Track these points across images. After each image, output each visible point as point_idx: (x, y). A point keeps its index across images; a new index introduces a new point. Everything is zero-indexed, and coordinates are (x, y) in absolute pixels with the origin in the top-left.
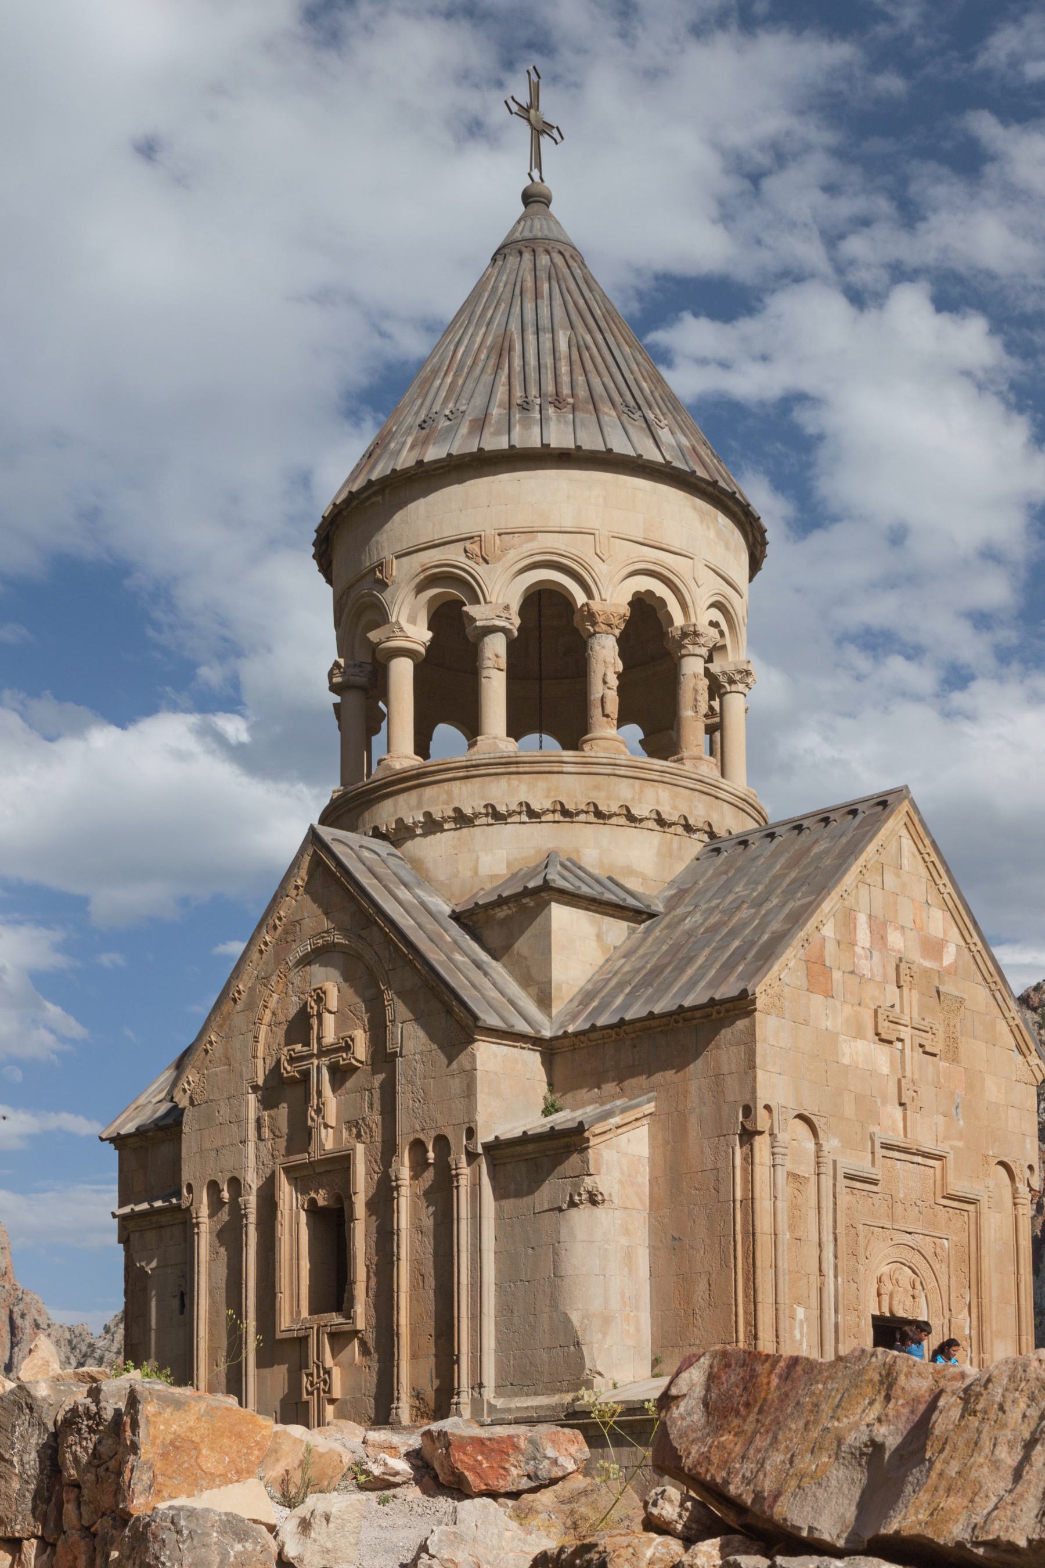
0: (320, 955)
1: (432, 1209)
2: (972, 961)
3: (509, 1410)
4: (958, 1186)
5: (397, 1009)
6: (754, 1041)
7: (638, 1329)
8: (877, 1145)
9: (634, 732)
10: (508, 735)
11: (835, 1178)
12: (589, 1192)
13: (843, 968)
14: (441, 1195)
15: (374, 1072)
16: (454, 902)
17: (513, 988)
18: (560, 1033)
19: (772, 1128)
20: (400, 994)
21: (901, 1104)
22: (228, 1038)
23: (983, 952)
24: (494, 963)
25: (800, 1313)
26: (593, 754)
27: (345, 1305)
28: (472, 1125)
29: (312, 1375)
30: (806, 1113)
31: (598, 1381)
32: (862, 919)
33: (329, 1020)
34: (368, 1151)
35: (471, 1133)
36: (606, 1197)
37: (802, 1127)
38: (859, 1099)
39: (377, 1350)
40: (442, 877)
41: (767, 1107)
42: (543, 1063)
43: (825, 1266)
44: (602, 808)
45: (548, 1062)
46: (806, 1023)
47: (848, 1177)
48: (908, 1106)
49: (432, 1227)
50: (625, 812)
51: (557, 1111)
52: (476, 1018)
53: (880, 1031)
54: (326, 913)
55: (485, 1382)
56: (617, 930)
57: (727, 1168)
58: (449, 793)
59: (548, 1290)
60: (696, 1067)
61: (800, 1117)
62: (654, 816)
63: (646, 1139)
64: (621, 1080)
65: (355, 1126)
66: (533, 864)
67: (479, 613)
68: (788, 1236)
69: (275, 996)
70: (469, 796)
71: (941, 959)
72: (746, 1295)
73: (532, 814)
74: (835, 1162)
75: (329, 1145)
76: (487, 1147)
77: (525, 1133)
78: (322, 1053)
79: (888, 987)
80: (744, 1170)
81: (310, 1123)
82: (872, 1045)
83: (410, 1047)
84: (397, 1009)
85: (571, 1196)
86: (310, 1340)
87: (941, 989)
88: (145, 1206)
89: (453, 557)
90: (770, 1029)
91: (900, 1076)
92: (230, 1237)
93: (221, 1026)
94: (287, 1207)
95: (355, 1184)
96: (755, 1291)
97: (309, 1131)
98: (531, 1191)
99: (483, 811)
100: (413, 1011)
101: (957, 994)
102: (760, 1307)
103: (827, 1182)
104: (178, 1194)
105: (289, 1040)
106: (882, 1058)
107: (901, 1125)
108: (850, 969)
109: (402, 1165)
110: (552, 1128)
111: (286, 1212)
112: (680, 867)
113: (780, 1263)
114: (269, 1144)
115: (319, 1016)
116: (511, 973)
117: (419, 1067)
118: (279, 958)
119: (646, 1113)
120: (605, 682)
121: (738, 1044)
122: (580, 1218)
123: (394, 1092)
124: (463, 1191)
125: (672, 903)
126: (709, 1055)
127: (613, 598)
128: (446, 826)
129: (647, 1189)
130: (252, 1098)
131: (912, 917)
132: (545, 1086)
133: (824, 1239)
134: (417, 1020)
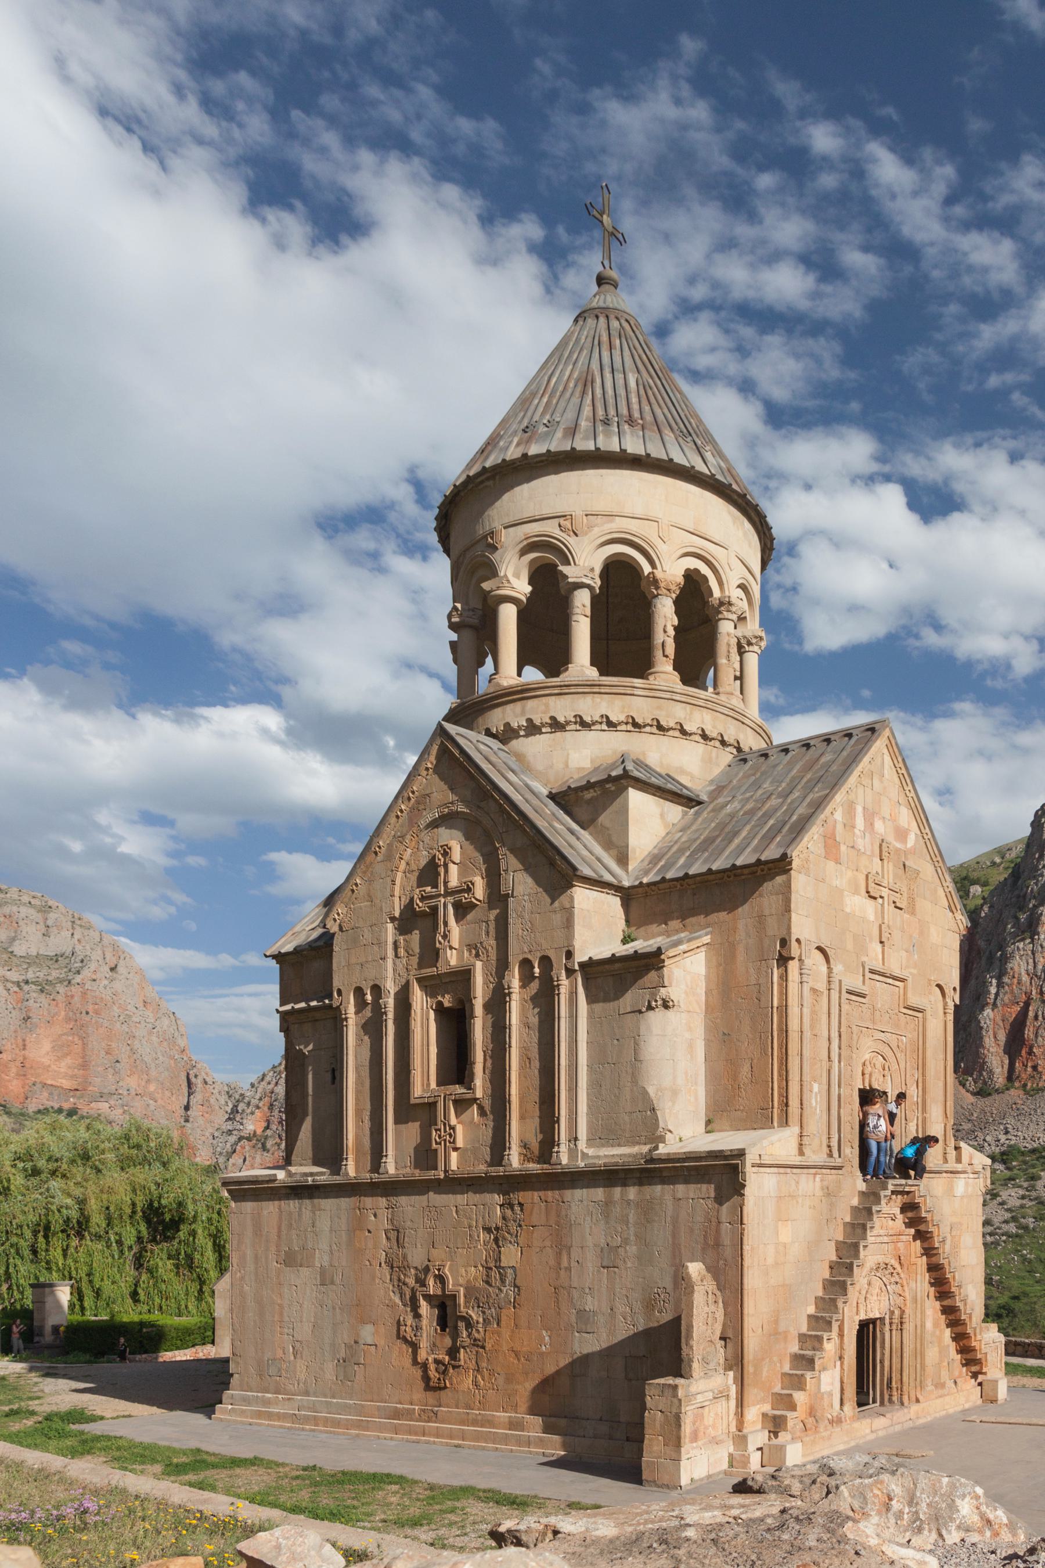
0: (446, 820)
1: (537, 1010)
3: (598, 1157)
4: (914, 1000)
5: (510, 862)
7: (696, 1099)
8: (867, 970)
10: (592, 664)
14: (545, 1000)
15: (490, 908)
16: (549, 786)
17: (598, 850)
18: (637, 883)
19: (801, 955)
20: (512, 851)
21: (881, 942)
22: (370, 881)
24: (582, 831)
25: (816, 1087)
27: (466, 1080)
28: (571, 948)
29: (440, 1130)
33: (453, 869)
35: (569, 955)
37: (819, 955)
39: (492, 1112)
41: (798, 941)
42: (622, 905)
45: (626, 904)
49: (537, 1024)
51: (633, 941)
54: (452, 789)
55: (579, 1136)
57: (767, 982)
58: (547, 705)
59: (630, 1071)
61: (819, 948)
63: (703, 962)
65: (475, 948)
66: (610, 762)
69: (409, 851)
70: (562, 708)
72: (780, 1075)
73: (610, 724)
74: (840, 981)
75: (453, 962)
77: (613, 955)
78: (448, 893)
80: (780, 985)
81: (438, 945)
83: (519, 890)
84: (510, 862)
85: (649, 1002)
86: (438, 1104)
88: (303, 1005)
90: (800, 882)
92: (373, 1028)
93: (365, 872)
94: (419, 1007)
95: (474, 991)
96: (787, 1072)
97: (437, 952)
98: (617, 998)
99: (573, 720)
100: (523, 864)
102: (790, 1083)
103: (835, 995)
104: (330, 996)
105: (421, 883)
106: (870, 909)
109: (513, 977)
110: (636, 952)
111: (419, 1011)
113: (804, 1052)
114: (404, 961)
115: (446, 866)
116: (596, 839)
118: (412, 822)
122: (656, 1018)
128: (544, 730)
129: (704, 998)
133: (832, 1035)
134: (526, 870)
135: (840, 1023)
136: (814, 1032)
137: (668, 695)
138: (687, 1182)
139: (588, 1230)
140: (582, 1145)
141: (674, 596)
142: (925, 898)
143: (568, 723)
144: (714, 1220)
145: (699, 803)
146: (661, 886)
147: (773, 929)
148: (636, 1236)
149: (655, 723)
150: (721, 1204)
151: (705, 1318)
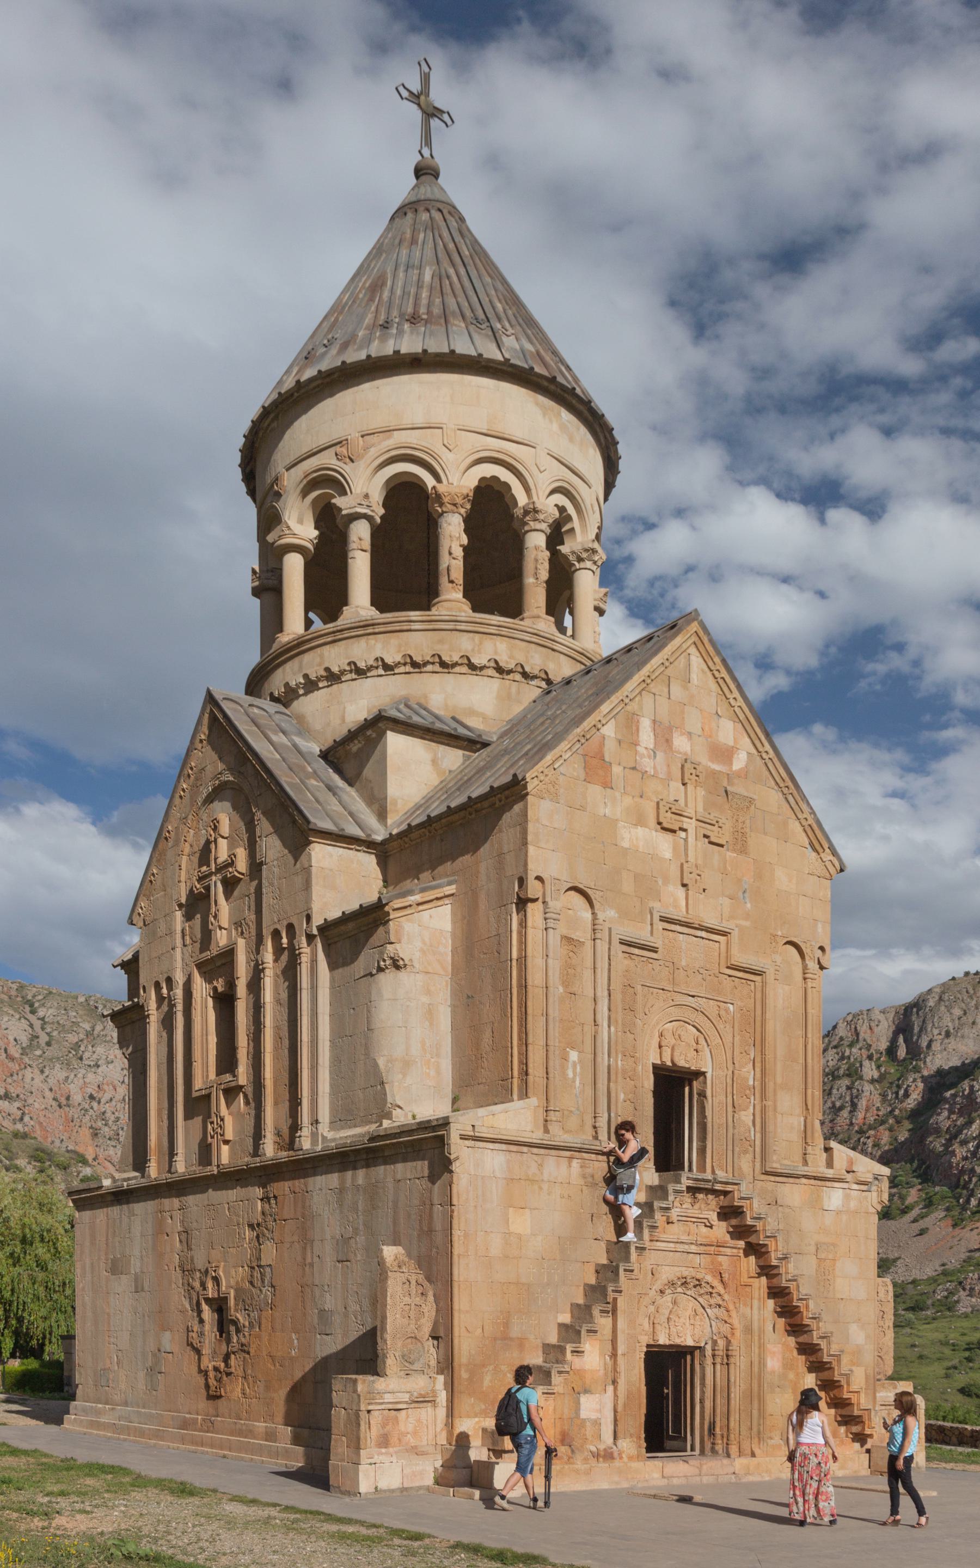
1: (287, 984)
2: (764, 768)
6: (526, 821)
7: (438, 1072)
11: (610, 943)
12: (391, 958)
15: (251, 880)
20: (264, 813)
21: (684, 885)
23: (775, 760)
26: (437, 613)
28: (309, 912)
30: (581, 886)
31: (396, 1113)
34: (247, 944)
36: (407, 962)
38: (637, 877)
39: (254, 1100)
42: (378, 864)
43: (599, 1017)
47: (622, 942)
48: (690, 887)
50: (466, 661)
52: (308, 822)
53: (661, 820)
57: (507, 931)
59: (363, 1042)
60: (484, 850)
62: (492, 664)
63: (449, 917)
64: (433, 868)
67: (344, 504)
68: (561, 989)
72: (520, 1039)
74: (610, 929)
76: (320, 929)
80: (519, 933)
81: (210, 927)
84: (264, 825)
89: (327, 461)
91: (683, 861)
94: (199, 995)
98: (352, 961)
103: (602, 946)
104: (138, 996)
106: (664, 845)
107: (684, 903)
111: (199, 1000)
113: (550, 1011)
117: (276, 870)
119: (447, 893)
120: (450, 554)
121: (515, 826)
122: (387, 980)
123: (261, 894)
124: (304, 966)
126: (494, 839)
129: (449, 958)
130: (179, 915)
132: (381, 883)
133: (599, 994)
135: (609, 979)
136: (574, 989)
137: (451, 626)
138: (405, 1160)
139: (326, 1223)
140: (324, 1129)
142: (765, 834)
144: (428, 1202)
145: (485, 745)
146: (413, 836)
147: (512, 870)
148: (364, 1225)
149: (437, 660)
150: (433, 1183)
151: (405, 1311)
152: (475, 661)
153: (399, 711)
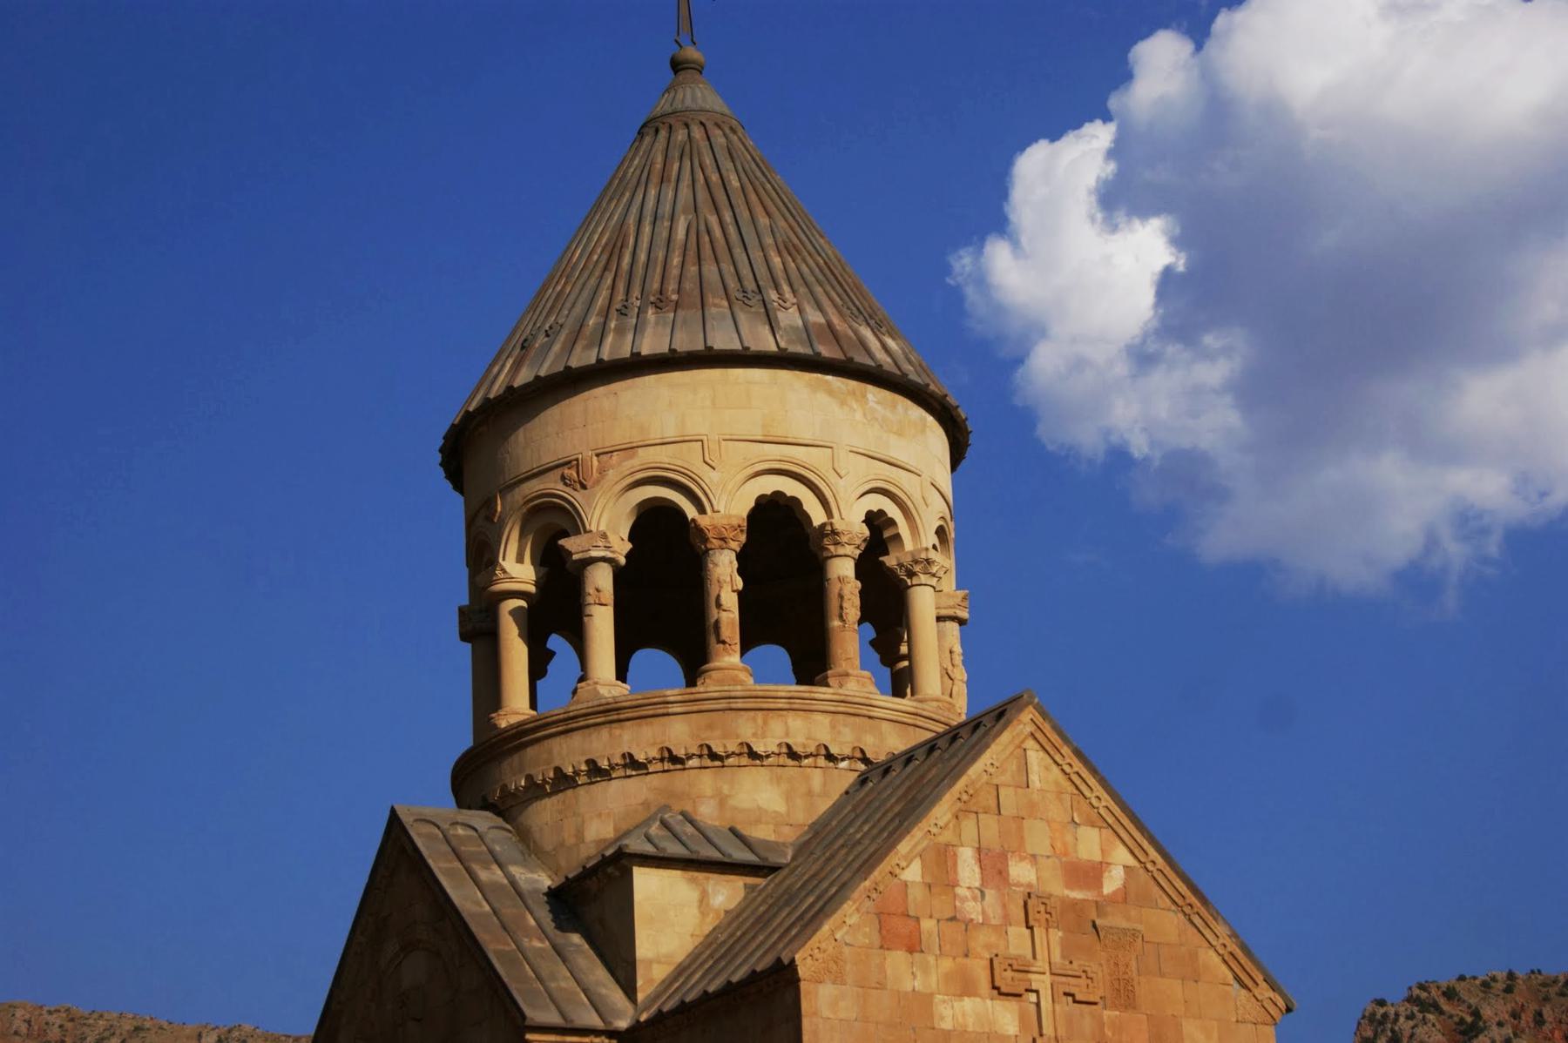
9: (776, 656)
13: (936, 915)
26: (701, 689)
32: (966, 856)
40: (548, 847)
44: (718, 749)
46: (881, 986)
52: (524, 1017)
56: (726, 893)
71: (1100, 886)
79: (1011, 930)
82: (989, 1002)
87: (1098, 922)
101: (1124, 924)
108: (950, 915)
112: (824, 806)
125: (803, 849)
127: (729, 504)
131: (1047, 842)
141: (736, 546)
143: (612, 767)
152: (759, 748)
153: (649, 839)
